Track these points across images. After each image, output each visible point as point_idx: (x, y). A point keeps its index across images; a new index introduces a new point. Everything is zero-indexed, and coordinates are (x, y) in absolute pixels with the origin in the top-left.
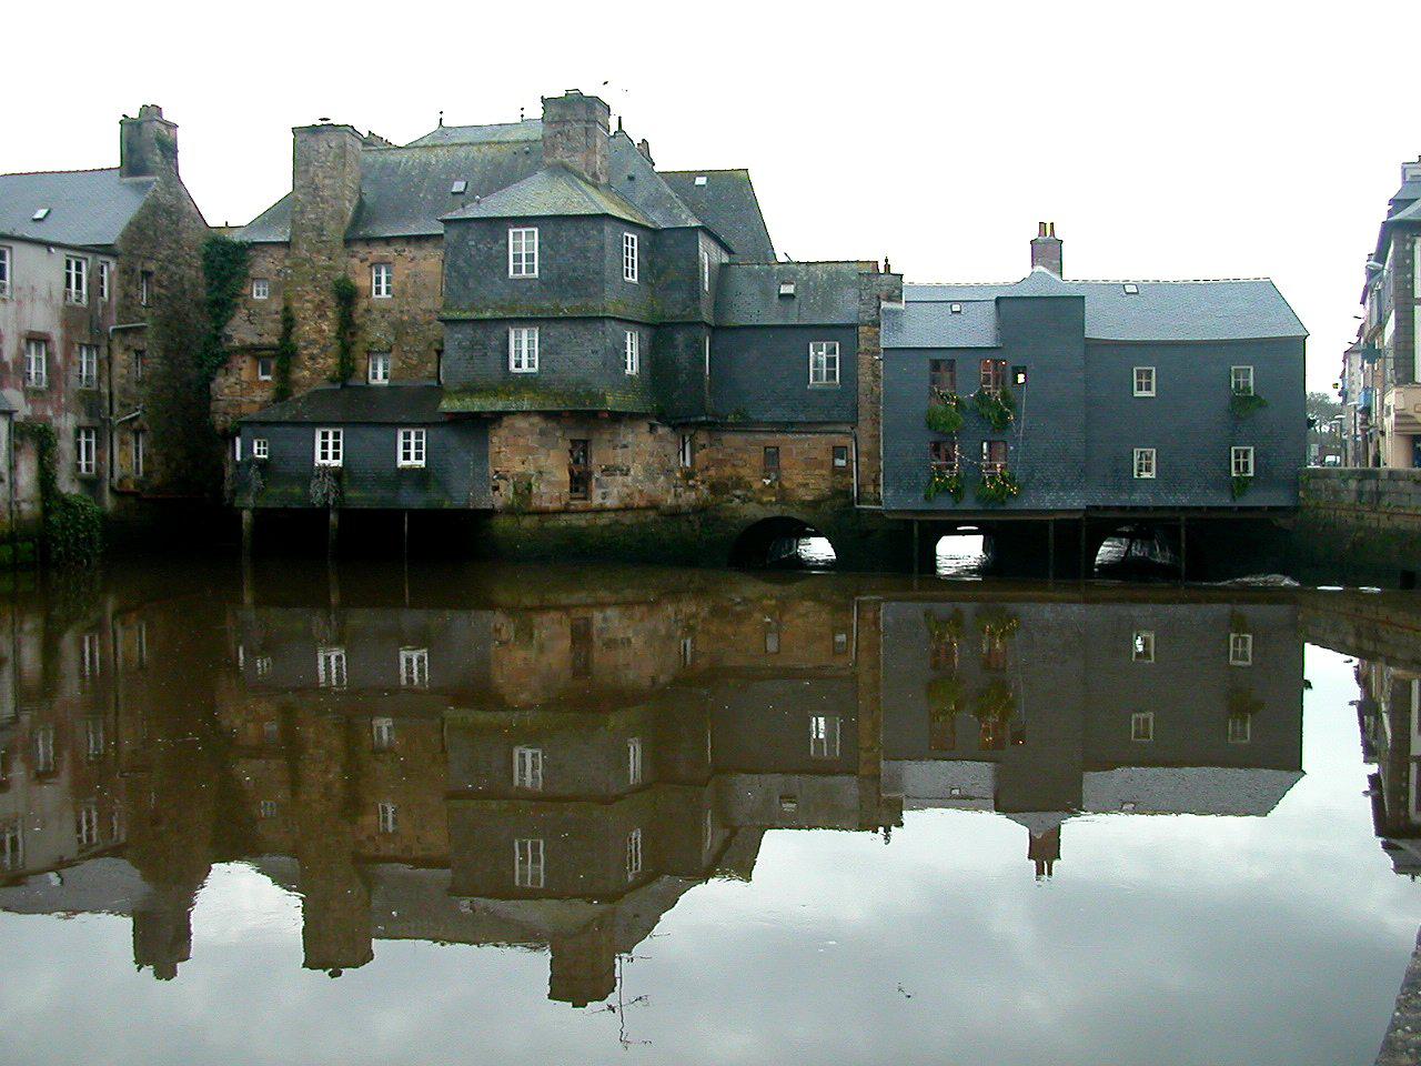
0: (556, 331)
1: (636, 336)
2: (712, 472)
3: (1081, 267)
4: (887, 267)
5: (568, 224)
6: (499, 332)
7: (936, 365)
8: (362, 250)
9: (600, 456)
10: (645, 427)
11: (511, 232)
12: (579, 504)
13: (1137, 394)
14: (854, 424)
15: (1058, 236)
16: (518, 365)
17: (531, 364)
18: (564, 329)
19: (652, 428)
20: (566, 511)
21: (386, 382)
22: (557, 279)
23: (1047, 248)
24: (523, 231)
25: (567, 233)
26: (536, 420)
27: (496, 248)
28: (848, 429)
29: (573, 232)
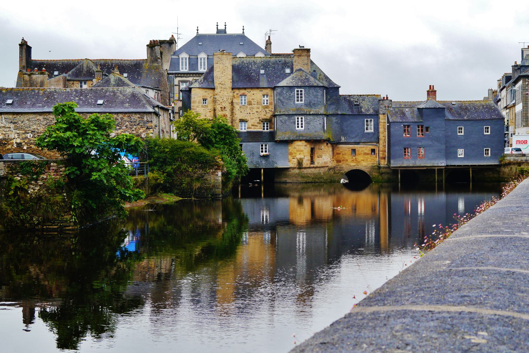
0: (309, 118)
1: (325, 118)
2: (336, 156)
3: (441, 97)
4: (387, 98)
5: (312, 88)
6: (292, 118)
7: (405, 126)
8: (237, 91)
9: (317, 152)
10: (325, 144)
11: (296, 90)
12: (312, 166)
13: (458, 134)
14: (378, 142)
15: (435, 89)
16: (298, 127)
17: (302, 127)
18: (311, 117)
19: (327, 144)
20: (309, 168)
21: (245, 131)
22: (309, 104)
23: (432, 92)
24: (299, 90)
25: (312, 91)
26: (304, 142)
27: (292, 94)
28: (375, 144)
29: (313, 91)
